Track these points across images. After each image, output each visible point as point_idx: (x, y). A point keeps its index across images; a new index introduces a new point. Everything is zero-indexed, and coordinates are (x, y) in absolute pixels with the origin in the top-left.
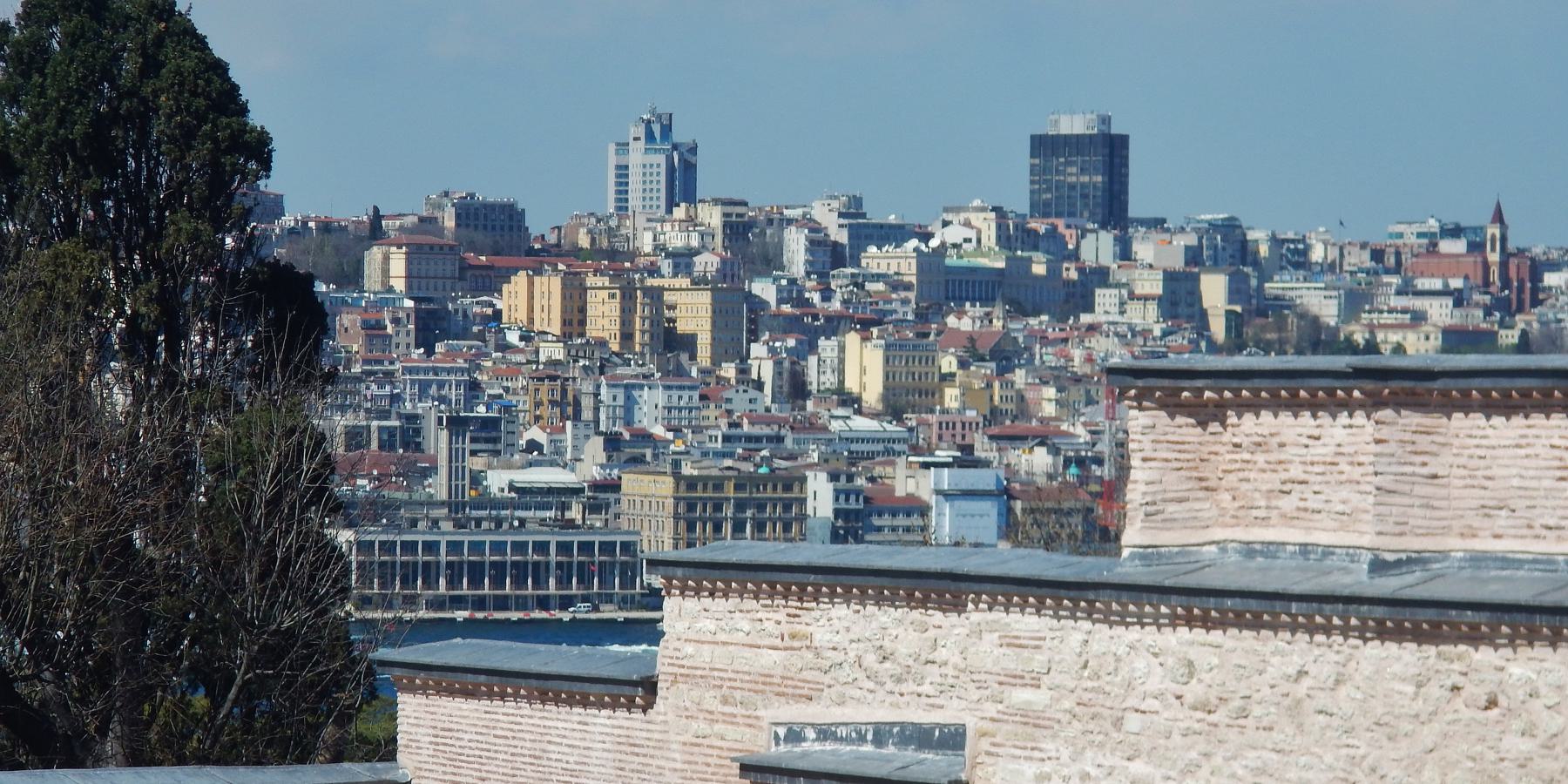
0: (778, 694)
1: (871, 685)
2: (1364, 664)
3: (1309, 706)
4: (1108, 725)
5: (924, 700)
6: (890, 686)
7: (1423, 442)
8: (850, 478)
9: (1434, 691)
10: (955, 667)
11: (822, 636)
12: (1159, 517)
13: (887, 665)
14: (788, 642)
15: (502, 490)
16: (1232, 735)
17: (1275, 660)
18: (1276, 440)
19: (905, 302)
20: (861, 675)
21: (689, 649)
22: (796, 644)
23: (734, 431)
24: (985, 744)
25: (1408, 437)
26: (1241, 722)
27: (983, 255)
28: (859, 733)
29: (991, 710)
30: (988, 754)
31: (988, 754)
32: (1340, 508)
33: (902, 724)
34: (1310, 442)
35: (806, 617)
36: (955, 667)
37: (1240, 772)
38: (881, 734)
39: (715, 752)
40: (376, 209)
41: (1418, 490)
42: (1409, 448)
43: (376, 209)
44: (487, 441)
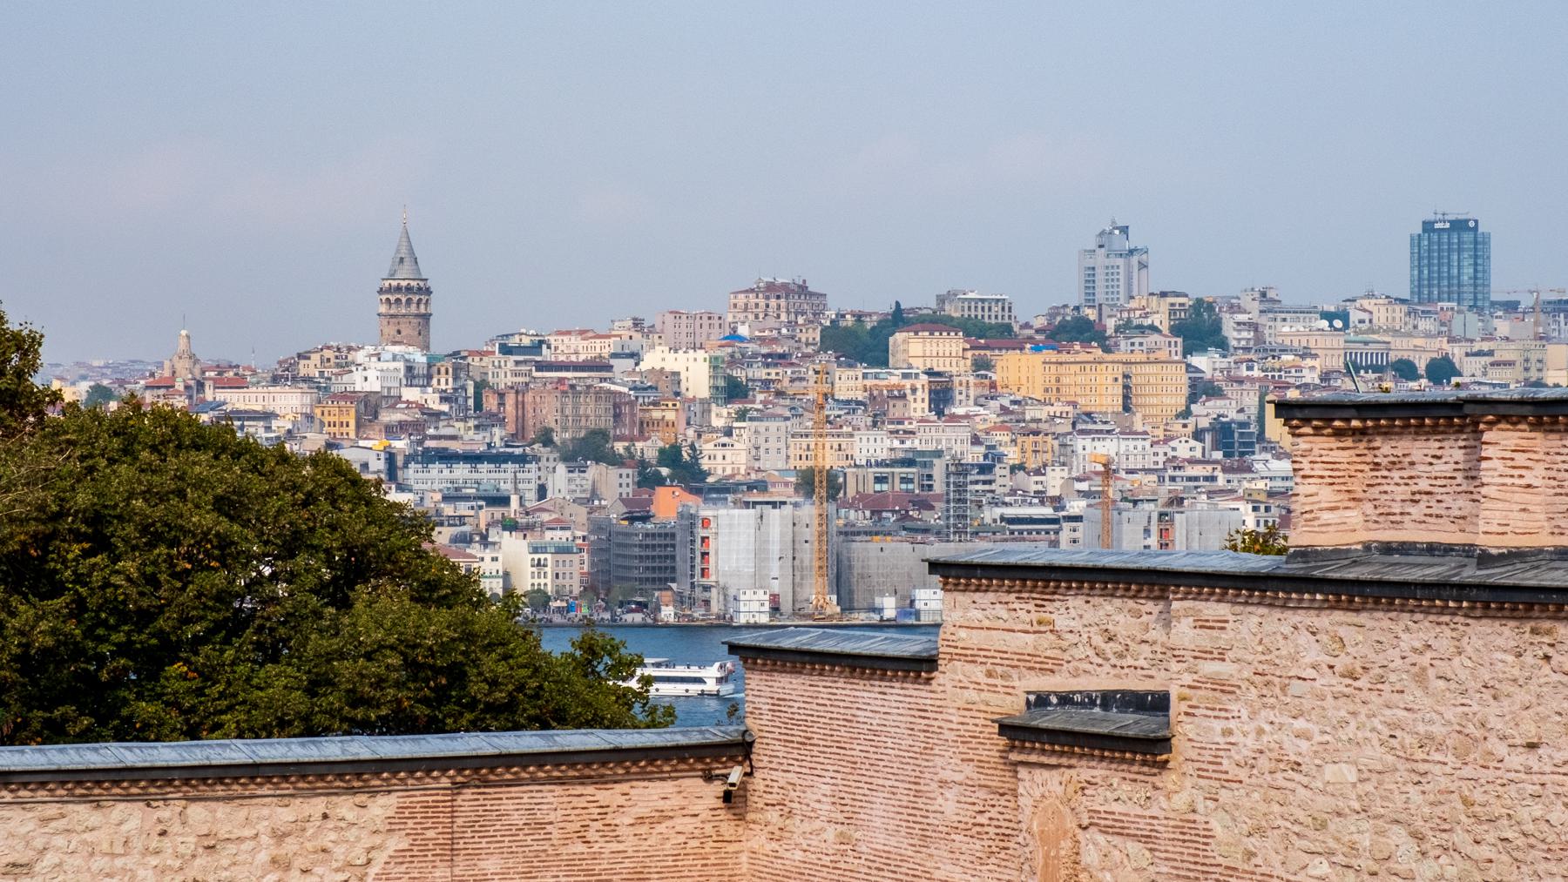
0: (1030, 668)
1: (1100, 661)
2: (1474, 638)
3: (1431, 672)
4: (1277, 691)
5: (1139, 672)
6: (1114, 661)
7: (1520, 459)
8: (1267, 509)
9: (1528, 659)
10: (1163, 645)
11: (1062, 622)
12: (1316, 523)
13: (1111, 644)
14: (1036, 627)
15: (995, 521)
16: (1373, 696)
17: (1404, 636)
18: (1408, 459)
19: (1313, 368)
20: (1091, 652)
21: (963, 633)
22: (1043, 628)
23: (1178, 473)
24: (1184, 707)
25: (1509, 454)
26: (1379, 686)
27: (1374, 332)
28: (1090, 697)
29: (1188, 679)
30: (1187, 714)
31: (1187, 714)
32: (1458, 513)
33: (1124, 693)
34: (1434, 461)
35: (1049, 607)
36: (1163, 645)
37: (1380, 727)
38: (1108, 699)
39: (982, 715)
40: (898, 304)
41: (1517, 497)
42: (1510, 463)
43: (898, 304)
44: (985, 482)
